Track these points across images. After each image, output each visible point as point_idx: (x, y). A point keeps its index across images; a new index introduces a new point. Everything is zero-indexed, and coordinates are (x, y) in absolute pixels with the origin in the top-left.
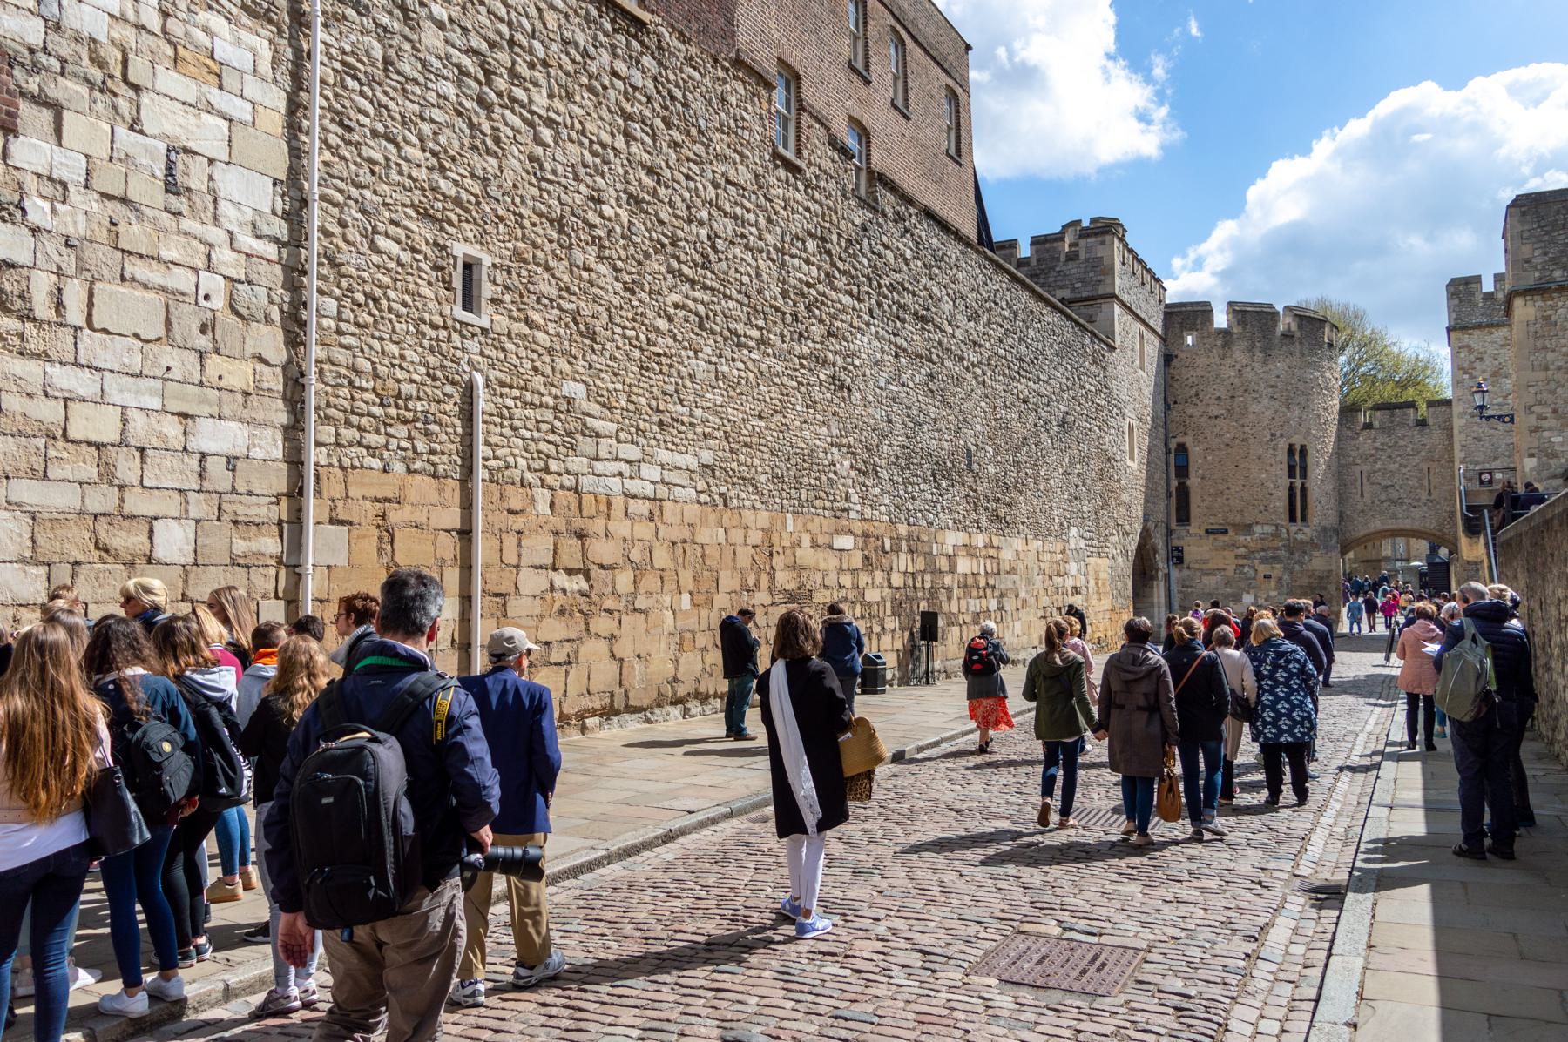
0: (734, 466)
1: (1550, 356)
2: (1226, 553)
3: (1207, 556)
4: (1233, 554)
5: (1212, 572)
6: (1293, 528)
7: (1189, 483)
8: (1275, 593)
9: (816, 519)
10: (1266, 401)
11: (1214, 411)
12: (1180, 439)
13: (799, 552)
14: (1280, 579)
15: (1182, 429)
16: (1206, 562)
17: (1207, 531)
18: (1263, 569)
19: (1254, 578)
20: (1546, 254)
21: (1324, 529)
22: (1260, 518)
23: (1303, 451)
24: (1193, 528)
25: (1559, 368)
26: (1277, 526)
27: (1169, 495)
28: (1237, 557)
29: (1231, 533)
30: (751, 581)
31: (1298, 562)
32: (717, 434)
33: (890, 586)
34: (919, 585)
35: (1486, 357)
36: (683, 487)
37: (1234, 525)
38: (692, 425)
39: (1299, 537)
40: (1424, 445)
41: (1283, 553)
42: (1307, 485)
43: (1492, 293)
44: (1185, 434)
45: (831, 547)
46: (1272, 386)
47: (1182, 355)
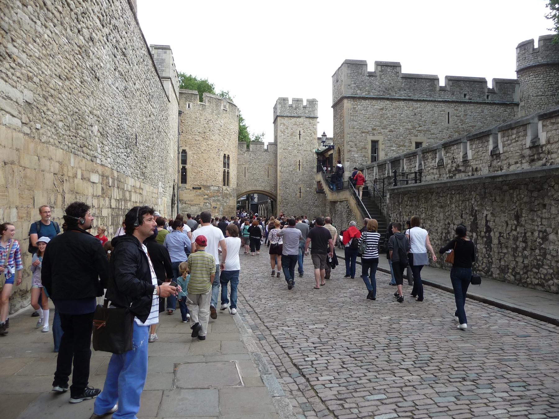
0: (45, 109)
1: (355, 123)
2: (200, 197)
3: (193, 198)
5: (195, 205)
6: (224, 188)
8: (218, 214)
9: (84, 161)
10: (217, 136)
12: (184, 148)
13: (76, 181)
15: (184, 143)
16: (192, 201)
17: (193, 188)
19: (210, 208)
20: (355, 83)
21: (234, 189)
22: (213, 183)
23: (228, 157)
24: (189, 185)
25: (358, 128)
26: (218, 187)
27: (179, 172)
28: (204, 199)
29: (202, 189)
30: (53, 201)
31: (225, 202)
32: (35, 79)
33: (111, 207)
34: (120, 207)
35: (289, 128)
36: (13, 116)
37: (204, 186)
38: (20, 65)
40: (267, 159)
41: (220, 198)
42: (229, 171)
43: (292, 105)
45: (89, 180)
46: (219, 130)
47: (186, 112)
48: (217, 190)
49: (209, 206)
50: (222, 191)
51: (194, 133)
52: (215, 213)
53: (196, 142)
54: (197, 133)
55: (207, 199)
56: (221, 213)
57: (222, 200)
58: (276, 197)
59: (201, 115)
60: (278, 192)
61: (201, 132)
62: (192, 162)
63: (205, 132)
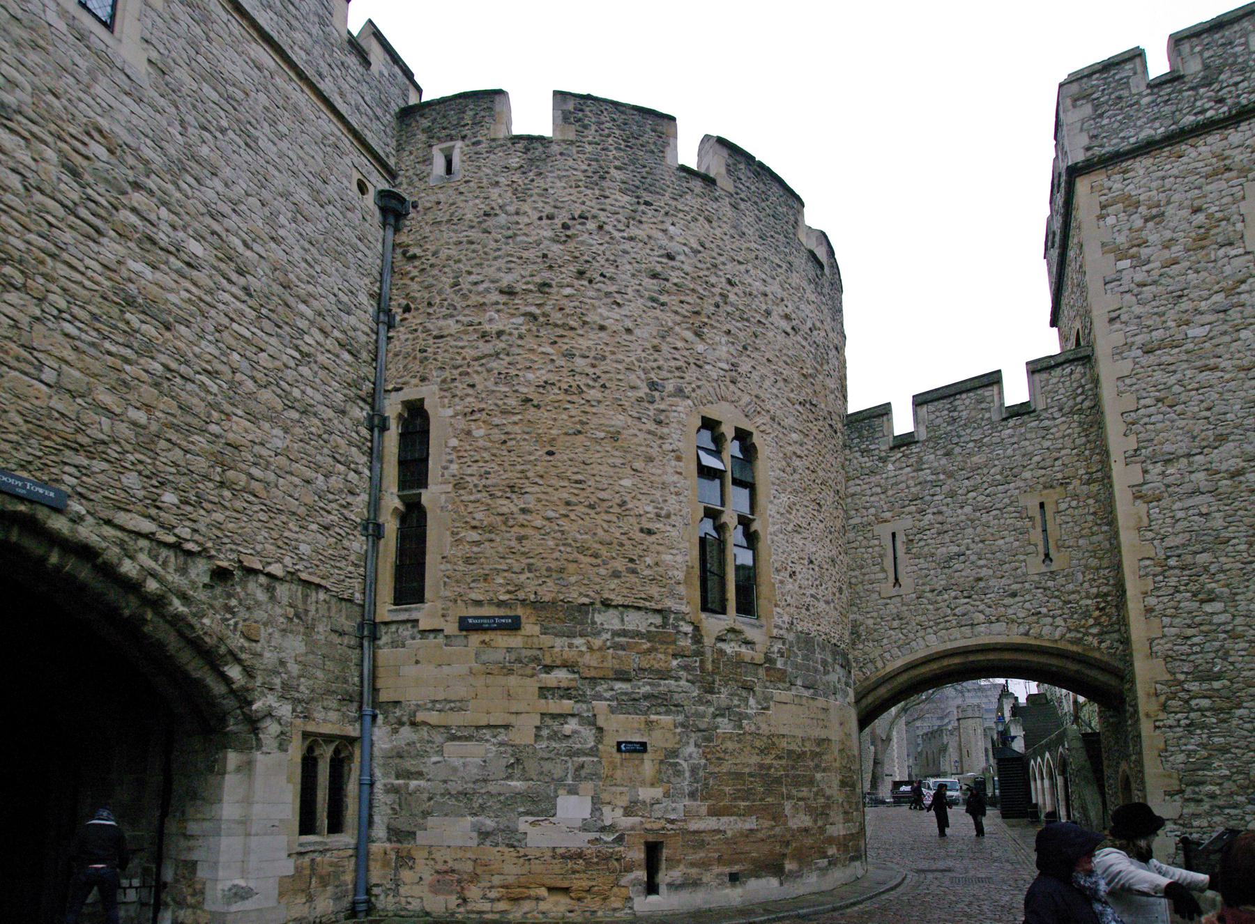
2: (513, 680)
3: (460, 691)
4: (532, 685)
7: (425, 500)
8: (658, 792)
11: (497, 321)
14: (674, 753)
16: (459, 705)
18: (623, 726)
19: (593, 752)
28: (544, 691)
31: (721, 712)
37: (537, 605)
39: (729, 648)
41: (682, 687)
44: (423, 379)
48: (649, 636)
49: (588, 734)
50: (697, 636)
51: (474, 299)
52: (633, 783)
53: (486, 348)
54: (495, 297)
55: (566, 692)
56: (685, 784)
57: (700, 701)
58: (1124, 674)
59: (521, 194)
60: (1138, 629)
61: (520, 287)
62: (454, 468)
63: (544, 286)
